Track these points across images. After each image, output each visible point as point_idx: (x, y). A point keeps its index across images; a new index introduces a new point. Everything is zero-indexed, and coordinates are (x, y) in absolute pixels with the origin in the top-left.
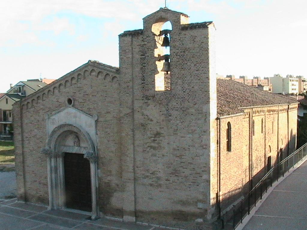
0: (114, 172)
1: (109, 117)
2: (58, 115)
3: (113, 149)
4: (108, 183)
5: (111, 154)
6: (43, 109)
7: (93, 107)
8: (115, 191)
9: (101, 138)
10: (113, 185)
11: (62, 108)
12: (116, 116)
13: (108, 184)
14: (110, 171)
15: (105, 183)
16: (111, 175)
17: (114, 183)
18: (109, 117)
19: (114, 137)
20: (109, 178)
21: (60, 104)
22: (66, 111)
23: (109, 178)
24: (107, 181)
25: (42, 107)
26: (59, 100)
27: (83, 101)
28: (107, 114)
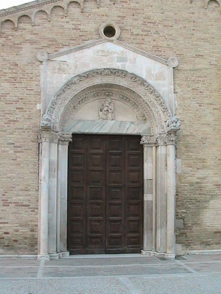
0: (210, 162)
1: (201, 64)
2: (78, 54)
3: (210, 119)
4: (197, 183)
5: (207, 129)
6: (32, 42)
7: (165, 45)
8: (213, 197)
9: (184, 99)
10: (209, 186)
11: (86, 43)
12: (216, 63)
13: (198, 186)
14: (203, 161)
15: (191, 184)
16: (204, 167)
17: (211, 183)
18: (201, 64)
19: (213, 98)
20: (201, 173)
21: (81, 34)
22: (99, 47)
23: (201, 173)
24: (194, 180)
25: (28, 37)
26: (81, 27)
27: (142, 33)
28: (198, 59)
